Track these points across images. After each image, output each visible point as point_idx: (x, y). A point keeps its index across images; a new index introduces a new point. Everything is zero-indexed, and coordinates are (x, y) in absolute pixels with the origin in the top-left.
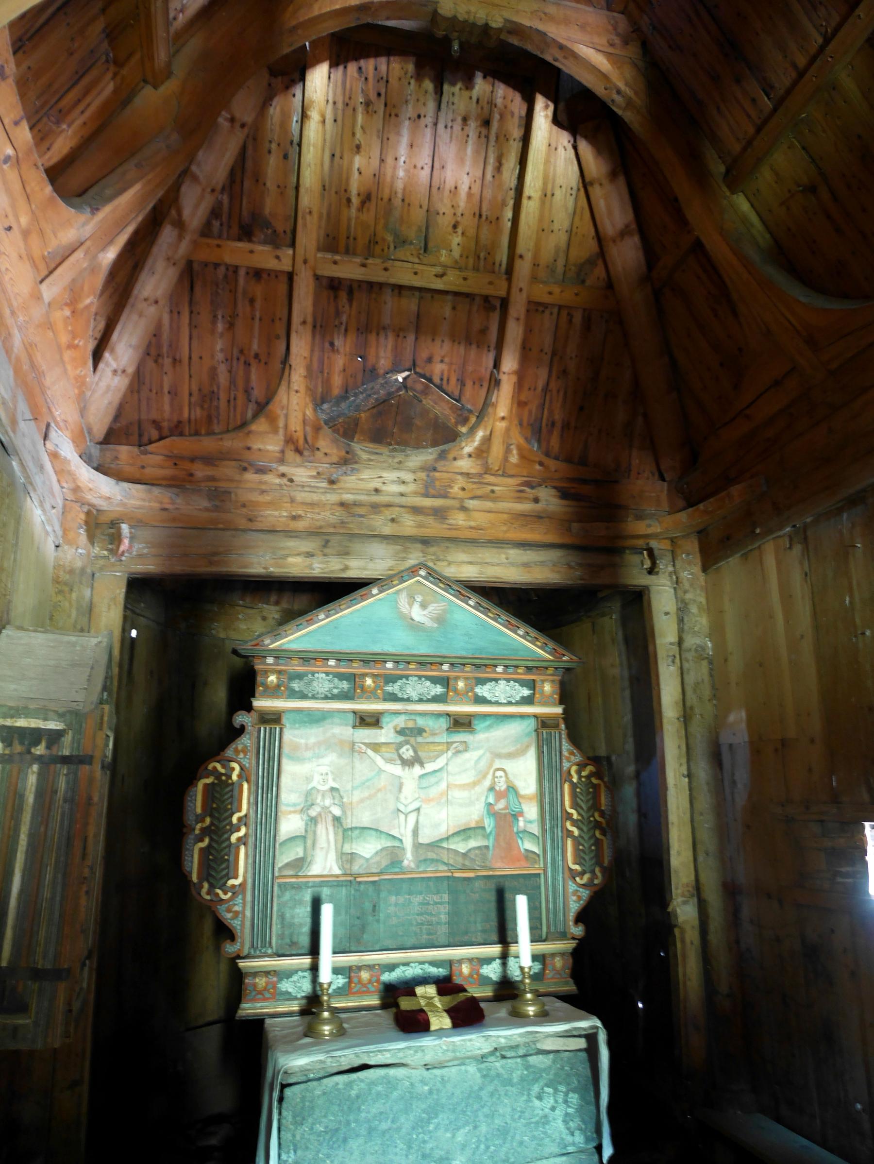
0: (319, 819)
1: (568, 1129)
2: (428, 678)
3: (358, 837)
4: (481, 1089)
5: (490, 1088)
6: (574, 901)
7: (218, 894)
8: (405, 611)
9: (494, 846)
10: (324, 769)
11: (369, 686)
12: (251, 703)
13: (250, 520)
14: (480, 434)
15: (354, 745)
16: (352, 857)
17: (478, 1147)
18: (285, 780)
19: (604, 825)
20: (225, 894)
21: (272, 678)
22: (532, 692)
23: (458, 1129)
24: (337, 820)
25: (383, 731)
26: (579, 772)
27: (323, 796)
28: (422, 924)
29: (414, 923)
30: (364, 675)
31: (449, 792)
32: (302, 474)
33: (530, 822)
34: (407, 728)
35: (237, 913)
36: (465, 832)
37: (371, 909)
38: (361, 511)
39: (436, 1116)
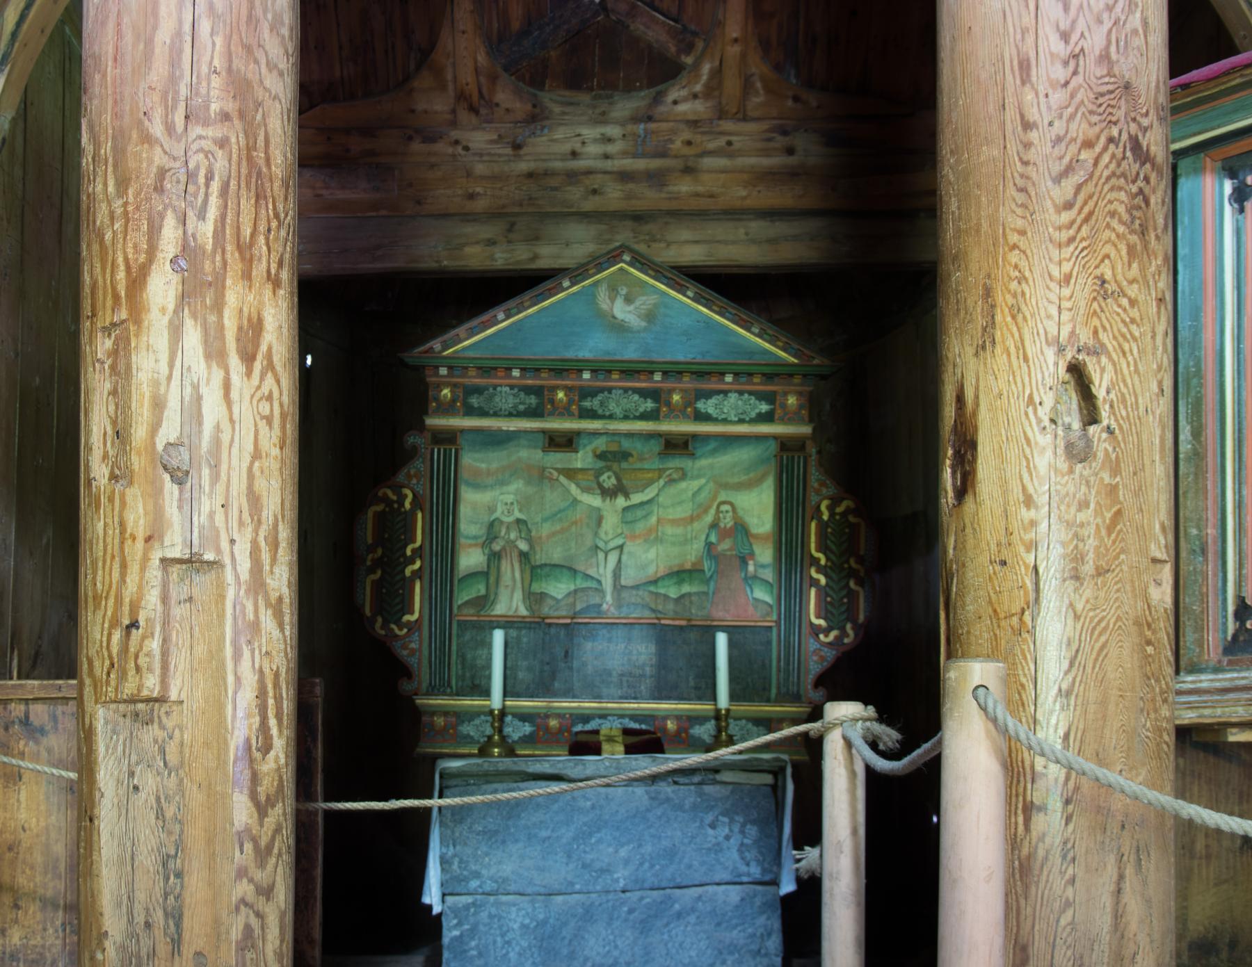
0: (504, 554)
1: (743, 858)
2: (635, 391)
3: (549, 576)
4: (648, 810)
5: (659, 812)
6: (815, 662)
7: (393, 630)
10: (510, 498)
11: (561, 400)
12: (423, 421)
13: (419, 203)
15: (544, 471)
16: (543, 596)
17: (641, 864)
18: (464, 511)
19: (862, 574)
20: (401, 629)
21: (446, 392)
22: (772, 407)
23: (622, 846)
24: (524, 556)
25: (580, 455)
26: (828, 508)
27: (508, 528)
28: (622, 675)
29: (614, 673)
30: (554, 389)
31: (660, 528)
32: (479, 139)
33: (763, 566)
34: (610, 452)
35: (413, 651)
36: (680, 575)
37: (563, 654)
38: (554, 182)
39: (599, 830)
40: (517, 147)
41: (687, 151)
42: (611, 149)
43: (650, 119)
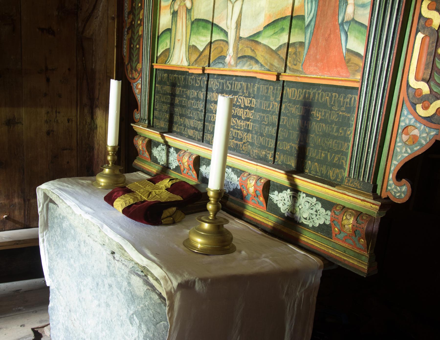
0: (179, 12)
9: (310, 43)
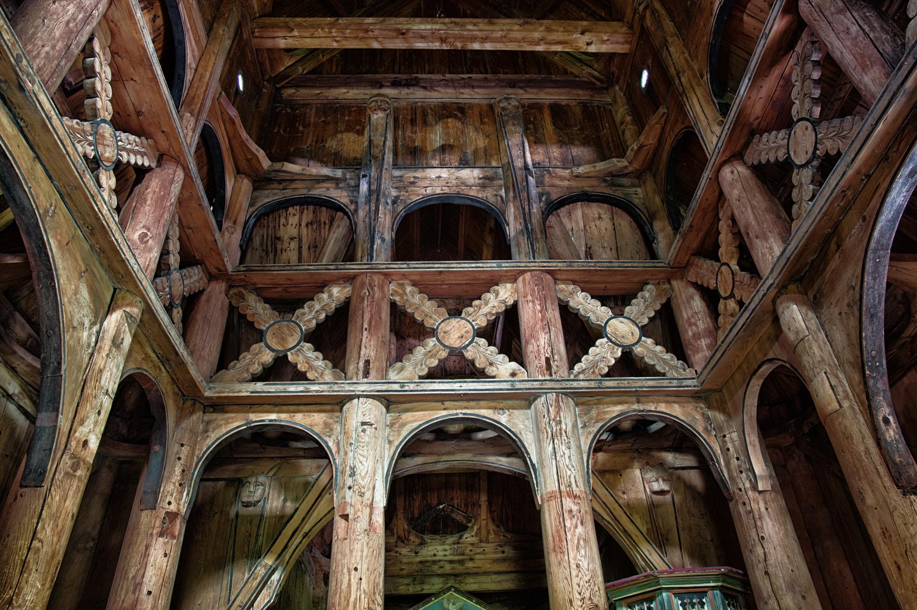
8: (446, 606)
14: (475, 528)
32: (404, 551)
38: (428, 564)
40: (416, 553)
41: (471, 553)
42: (446, 553)
43: (459, 543)
